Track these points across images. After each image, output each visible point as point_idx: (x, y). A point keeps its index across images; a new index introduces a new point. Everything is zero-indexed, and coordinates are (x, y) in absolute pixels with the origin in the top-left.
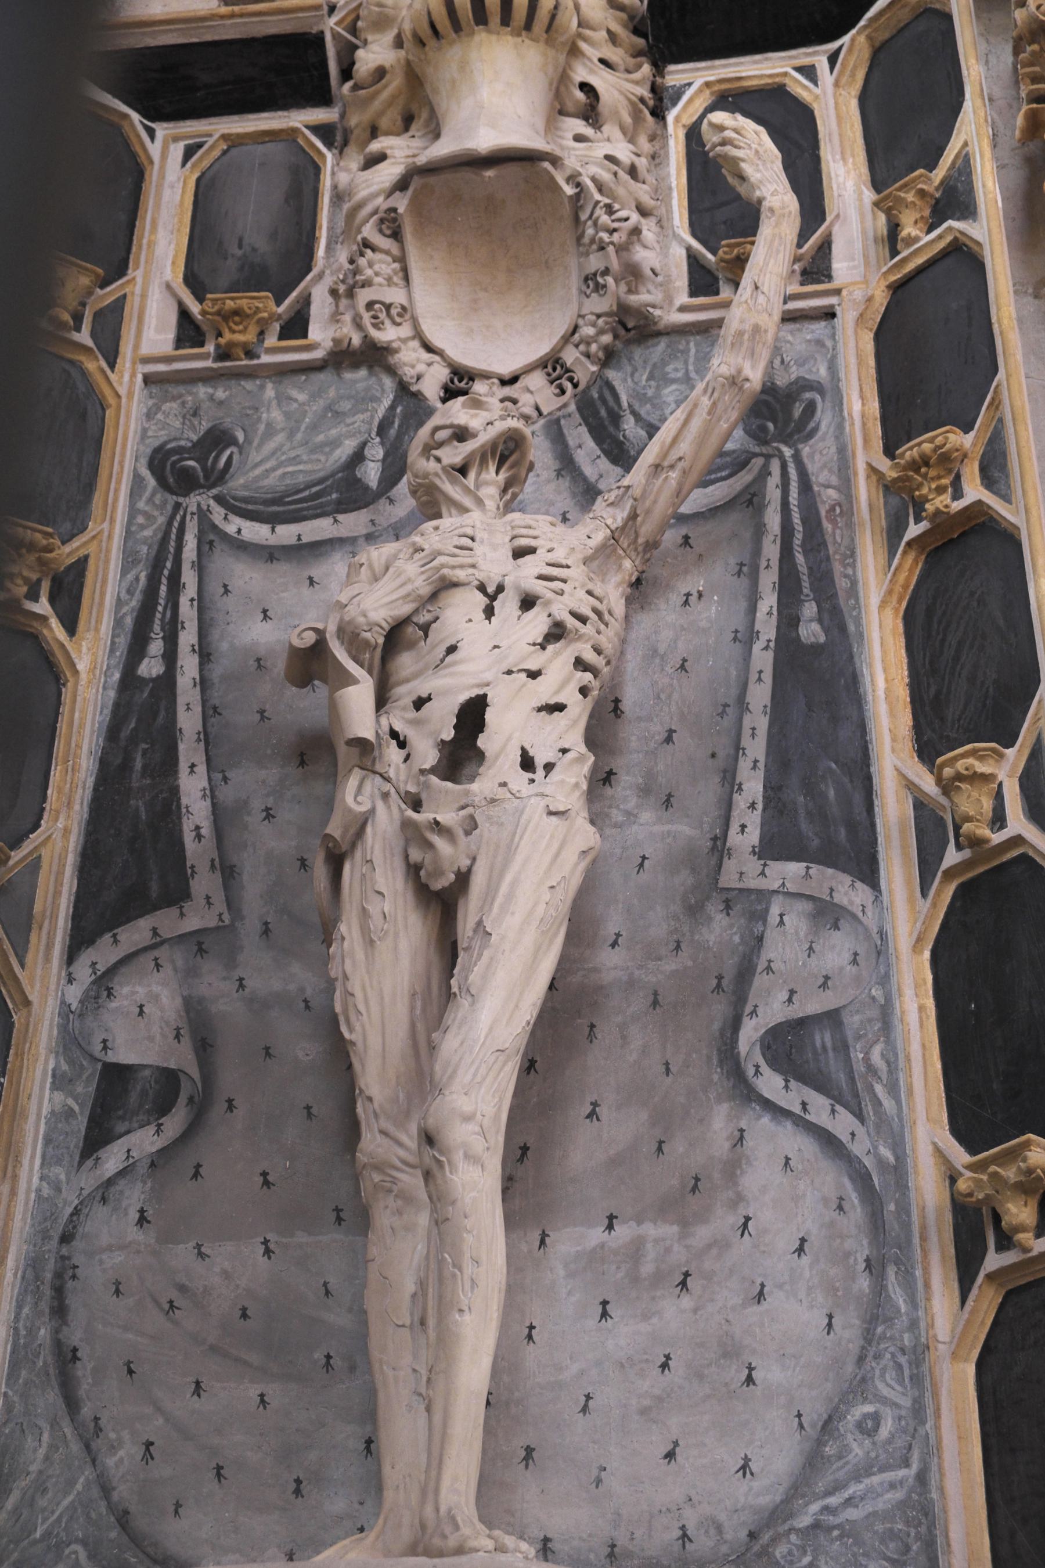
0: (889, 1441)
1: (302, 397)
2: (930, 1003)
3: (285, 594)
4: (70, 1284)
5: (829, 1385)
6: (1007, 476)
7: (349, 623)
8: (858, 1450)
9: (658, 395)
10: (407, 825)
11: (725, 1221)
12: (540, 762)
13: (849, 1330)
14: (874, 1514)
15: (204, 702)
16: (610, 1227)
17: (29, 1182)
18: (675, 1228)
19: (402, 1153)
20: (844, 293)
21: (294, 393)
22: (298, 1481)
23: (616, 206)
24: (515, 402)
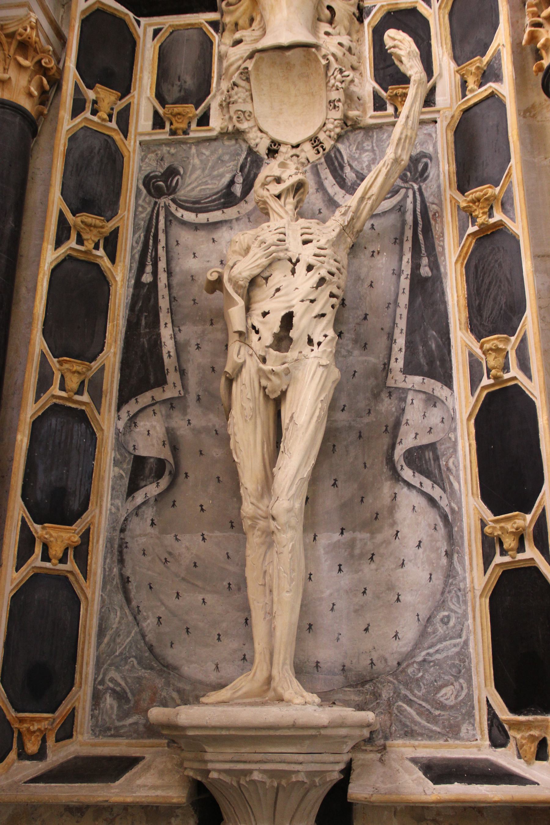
0: (454, 627)
1: (207, 153)
2: (474, 443)
3: (202, 246)
4: (125, 550)
5: (430, 603)
6: (514, 209)
7: (234, 277)
8: (441, 630)
9: (360, 157)
10: (260, 370)
11: (388, 533)
12: (315, 342)
13: (438, 580)
14: (448, 656)
15: (170, 295)
16: (342, 533)
17: (107, 505)
18: (368, 535)
19: (260, 512)
20: (441, 112)
21: (204, 151)
22: (219, 635)
23: (344, 69)
24: (298, 156)
